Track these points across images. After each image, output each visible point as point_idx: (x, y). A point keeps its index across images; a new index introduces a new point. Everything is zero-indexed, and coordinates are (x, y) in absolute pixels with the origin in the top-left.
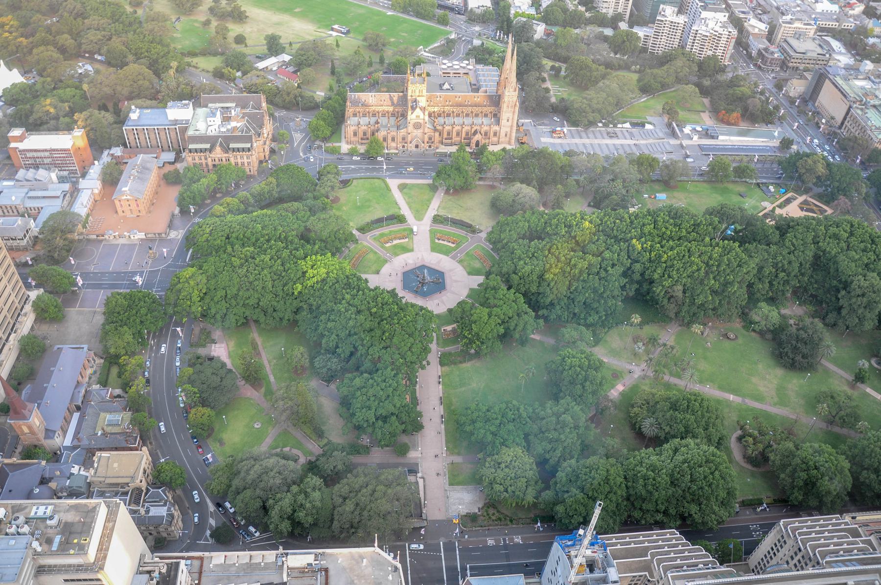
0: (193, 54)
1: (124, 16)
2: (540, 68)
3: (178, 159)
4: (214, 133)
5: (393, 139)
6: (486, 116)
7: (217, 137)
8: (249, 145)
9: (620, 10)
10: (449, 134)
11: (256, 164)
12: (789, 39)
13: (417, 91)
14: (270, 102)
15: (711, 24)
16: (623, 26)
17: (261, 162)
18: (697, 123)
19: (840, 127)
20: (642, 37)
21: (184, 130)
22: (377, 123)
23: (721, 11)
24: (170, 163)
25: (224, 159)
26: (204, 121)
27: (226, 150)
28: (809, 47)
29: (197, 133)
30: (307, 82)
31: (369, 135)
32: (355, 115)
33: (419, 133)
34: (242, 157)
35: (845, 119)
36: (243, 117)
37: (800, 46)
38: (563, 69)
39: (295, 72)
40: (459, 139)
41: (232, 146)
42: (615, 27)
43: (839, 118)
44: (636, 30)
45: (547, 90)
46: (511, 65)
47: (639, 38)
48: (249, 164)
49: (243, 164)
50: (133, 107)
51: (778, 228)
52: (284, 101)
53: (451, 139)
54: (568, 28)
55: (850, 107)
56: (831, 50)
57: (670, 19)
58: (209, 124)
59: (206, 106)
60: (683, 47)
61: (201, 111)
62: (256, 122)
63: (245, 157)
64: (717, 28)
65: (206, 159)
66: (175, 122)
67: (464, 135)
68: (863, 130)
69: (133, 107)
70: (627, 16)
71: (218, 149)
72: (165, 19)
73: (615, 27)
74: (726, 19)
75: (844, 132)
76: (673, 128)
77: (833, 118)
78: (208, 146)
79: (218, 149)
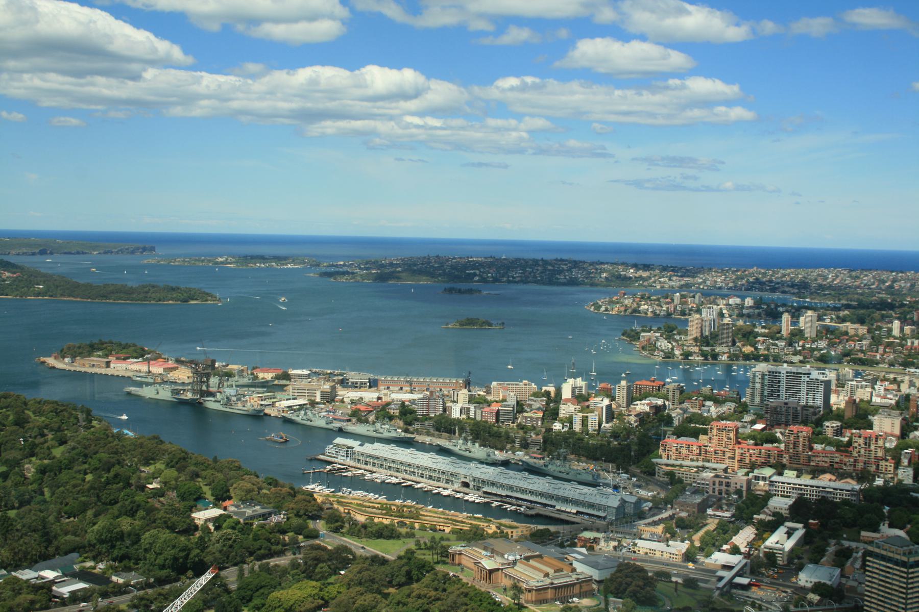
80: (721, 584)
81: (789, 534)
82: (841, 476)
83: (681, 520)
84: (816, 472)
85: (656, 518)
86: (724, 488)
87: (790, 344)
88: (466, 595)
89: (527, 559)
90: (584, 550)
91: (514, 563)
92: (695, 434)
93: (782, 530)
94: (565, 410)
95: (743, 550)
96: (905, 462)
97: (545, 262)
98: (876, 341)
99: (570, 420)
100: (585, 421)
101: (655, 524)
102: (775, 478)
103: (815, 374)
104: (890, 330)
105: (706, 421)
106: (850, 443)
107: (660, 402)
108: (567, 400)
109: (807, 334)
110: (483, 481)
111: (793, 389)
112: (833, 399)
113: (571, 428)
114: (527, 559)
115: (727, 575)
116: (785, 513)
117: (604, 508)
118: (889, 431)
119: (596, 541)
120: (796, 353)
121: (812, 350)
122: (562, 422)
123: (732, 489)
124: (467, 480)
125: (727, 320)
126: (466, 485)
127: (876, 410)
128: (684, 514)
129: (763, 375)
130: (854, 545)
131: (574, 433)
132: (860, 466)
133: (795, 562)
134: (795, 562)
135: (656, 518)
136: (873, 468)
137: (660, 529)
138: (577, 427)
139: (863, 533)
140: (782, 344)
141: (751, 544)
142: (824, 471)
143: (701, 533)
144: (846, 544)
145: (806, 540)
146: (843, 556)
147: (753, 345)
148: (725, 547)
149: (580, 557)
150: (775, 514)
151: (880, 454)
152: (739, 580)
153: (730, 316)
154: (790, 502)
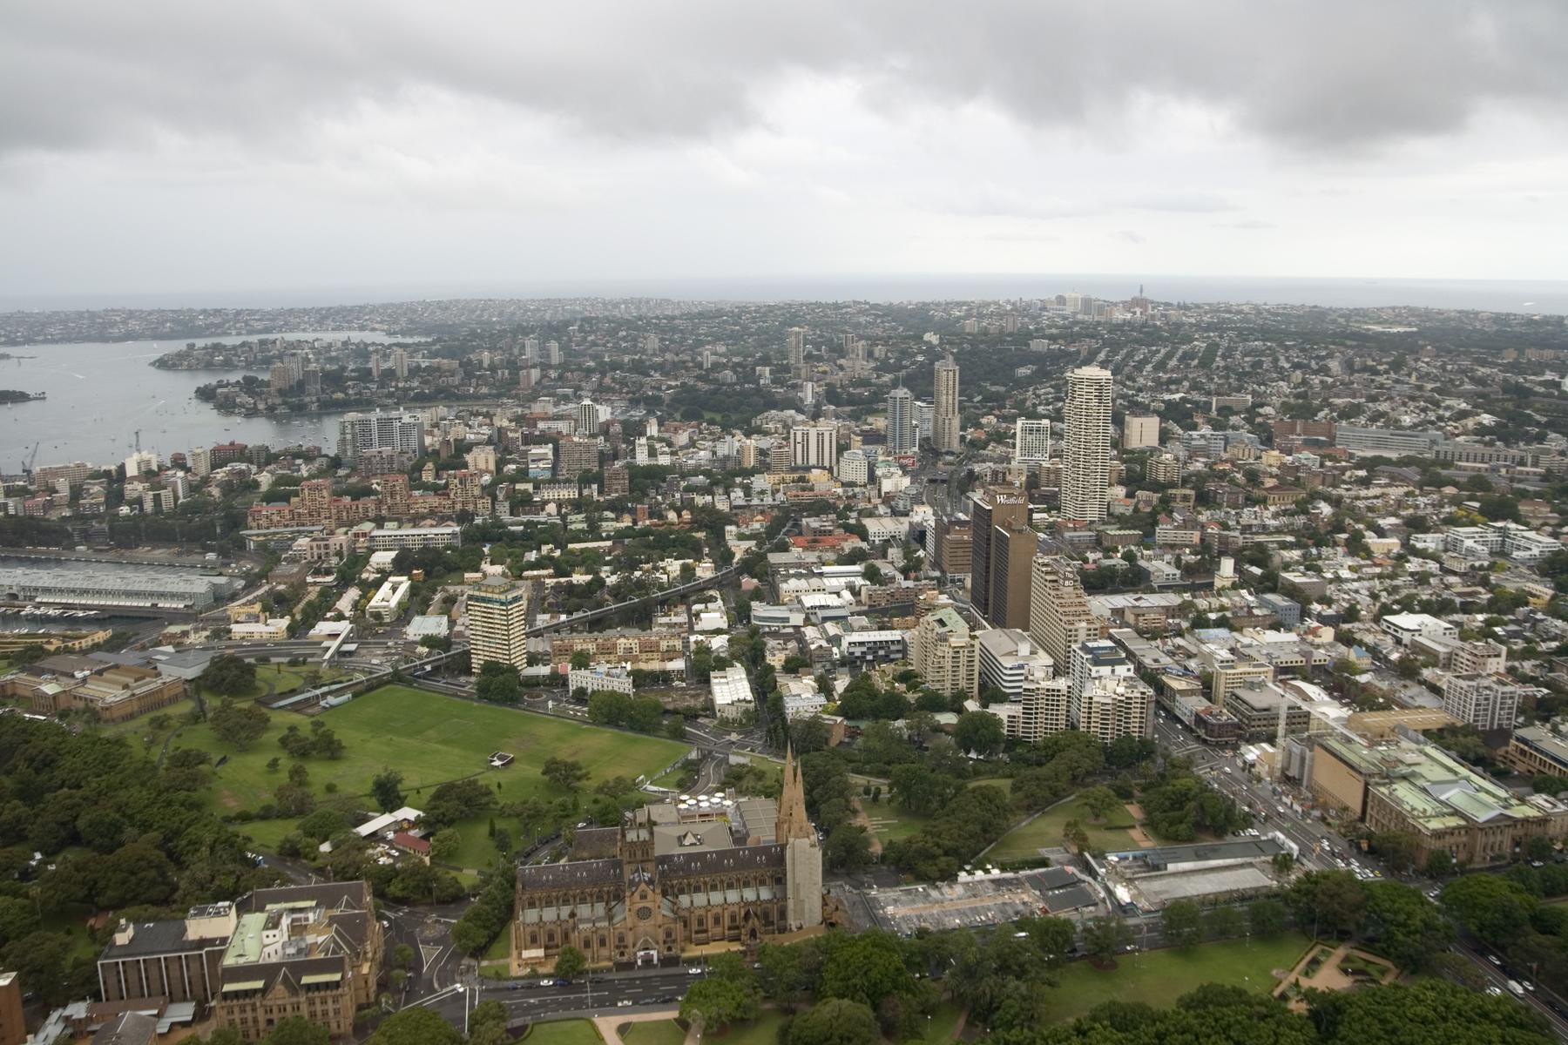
0: (245, 818)
1: (127, 760)
2: (844, 791)
3: (202, 1015)
4: (274, 959)
5: (603, 943)
6: (762, 883)
7: (275, 968)
8: (337, 977)
9: (963, 684)
10: (700, 922)
11: (351, 1012)
12: (1237, 691)
13: (639, 853)
14: (379, 894)
15: (1111, 685)
16: (972, 706)
17: (360, 1008)
18: (1124, 848)
19: (1362, 819)
20: (1005, 720)
21: (217, 956)
22: (572, 915)
23: (1121, 662)
24: (185, 1024)
25: (289, 1008)
26: (251, 937)
27: (294, 988)
28: (1274, 696)
29: (242, 961)
30: (446, 856)
31: (558, 939)
32: (532, 905)
33: (645, 926)
34: (324, 1002)
35: (1365, 804)
36: (329, 925)
37: (1256, 699)
38: (885, 789)
39: (425, 838)
40: (719, 930)
41: (306, 980)
42: (960, 710)
43: (1355, 804)
44: (994, 709)
45: (863, 829)
46: (795, 792)
47: (1000, 721)
48: (337, 1012)
49: (325, 1013)
50: (123, 921)
51: (1314, 1016)
52: (407, 891)
53: (706, 931)
54: (882, 721)
55: (1367, 784)
56: (1307, 698)
57: (1044, 684)
58: (266, 941)
59: (261, 909)
60: (1074, 727)
61: (255, 920)
62: (351, 930)
63: (330, 1001)
64: (1121, 690)
65: (254, 1010)
66: (202, 943)
67: (727, 922)
68: (1401, 817)
69: (123, 921)
70: (976, 690)
71: (279, 988)
72: (202, 759)
73: (960, 710)
74: (1131, 674)
75: (1369, 826)
76: (1087, 863)
77: (1346, 809)
78: (259, 984)
79: (279, 988)
80: (327, 656)
81: (394, 589)
82: (443, 520)
83: (280, 594)
84: (416, 520)
85: (250, 597)
86: (323, 551)
87: (382, 385)
88: (24, 731)
89: (100, 673)
90: (170, 649)
91: (84, 680)
92: (286, 498)
93: (386, 586)
94: (134, 489)
95: (347, 614)
96: (501, 497)
97: (92, 315)
98: (469, 375)
99: (139, 501)
100: (157, 499)
101: (251, 603)
102: (375, 533)
103: (406, 419)
104: (481, 362)
105: (297, 482)
106: (446, 486)
107: (243, 466)
108: (134, 478)
109: (399, 373)
110: (36, 589)
111: (385, 438)
112: (428, 440)
113: (142, 509)
114: (100, 673)
115: (334, 645)
116: (389, 567)
117: (191, 596)
118: (482, 466)
119: (185, 634)
120: (391, 395)
121: (405, 390)
122: (130, 504)
123: (332, 551)
124: (14, 591)
125: (313, 366)
126: (14, 596)
127: (469, 448)
128: (282, 587)
129: (353, 424)
130: (459, 589)
131: (146, 515)
132: (458, 507)
133: (405, 613)
134: (405, 613)
135: (250, 597)
136: (470, 508)
137: (257, 607)
138: (149, 506)
139: (467, 575)
140: (374, 386)
141: (356, 605)
142: (424, 517)
143: (301, 606)
144: (451, 589)
145: (414, 591)
146: (450, 601)
147: (344, 390)
148: (329, 615)
149: (163, 658)
150: (379, 571)
151: (477, 492)
152: (347, 647)
153: (317, 360)
154: (393, 554)
